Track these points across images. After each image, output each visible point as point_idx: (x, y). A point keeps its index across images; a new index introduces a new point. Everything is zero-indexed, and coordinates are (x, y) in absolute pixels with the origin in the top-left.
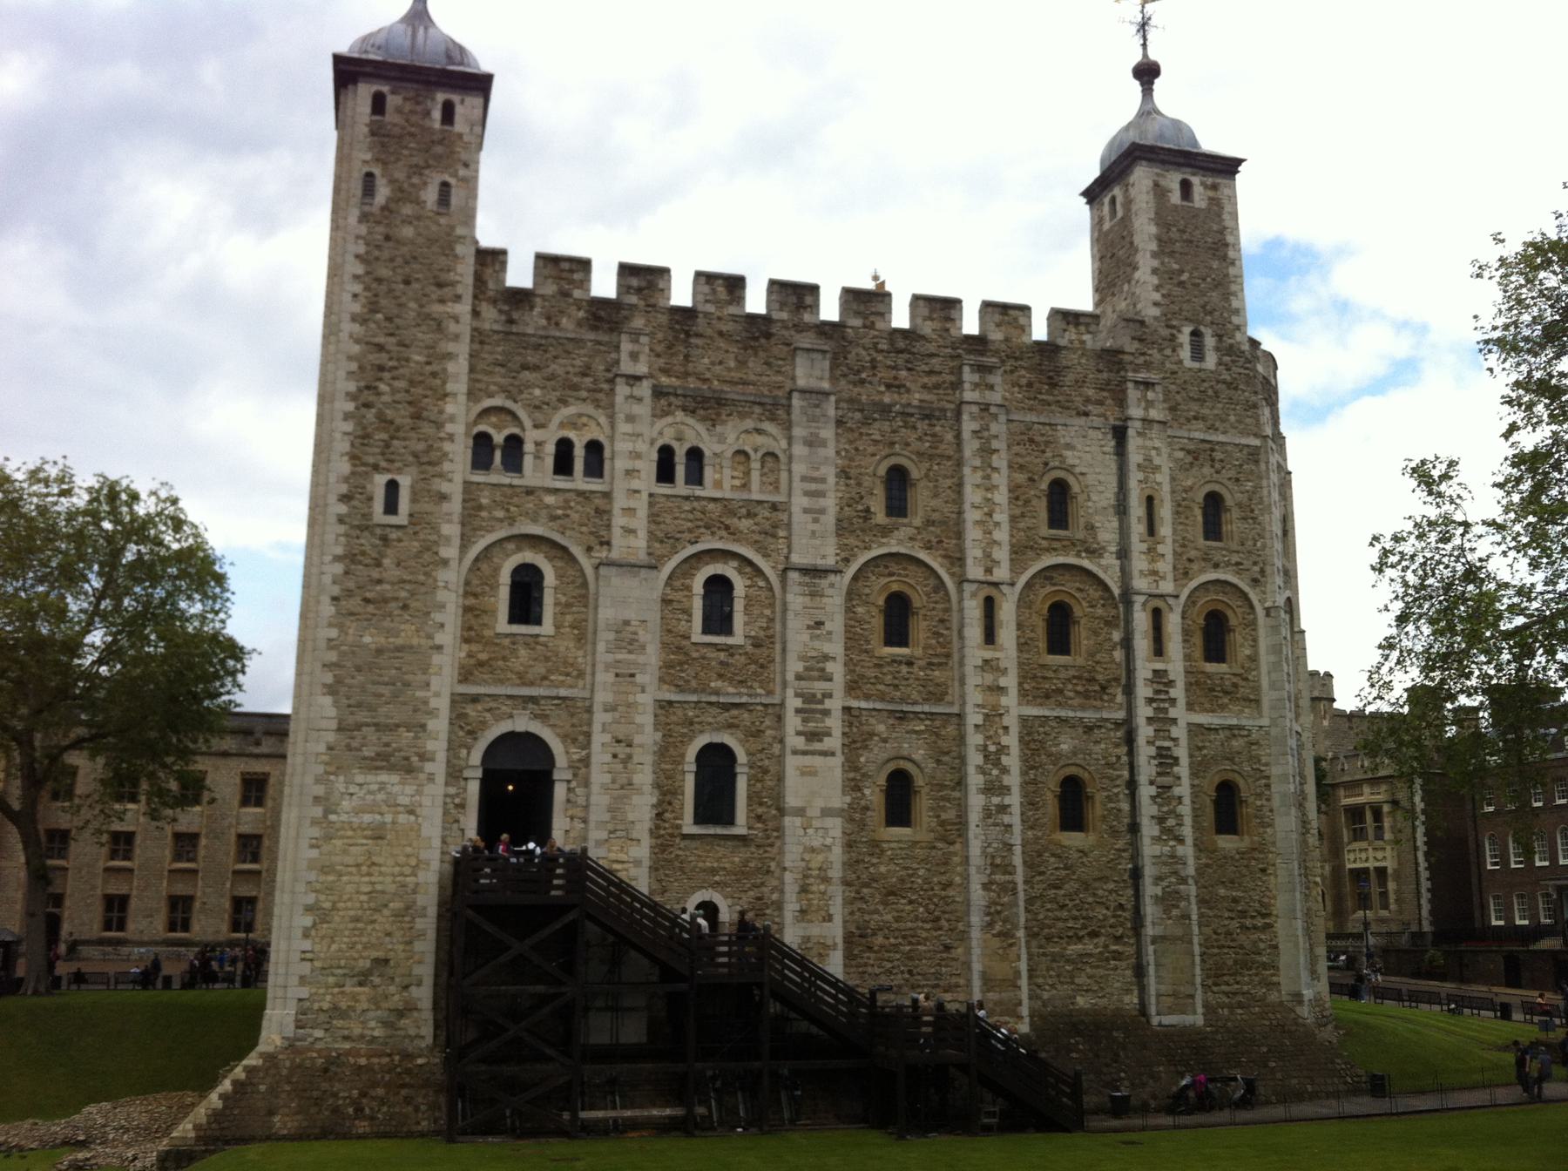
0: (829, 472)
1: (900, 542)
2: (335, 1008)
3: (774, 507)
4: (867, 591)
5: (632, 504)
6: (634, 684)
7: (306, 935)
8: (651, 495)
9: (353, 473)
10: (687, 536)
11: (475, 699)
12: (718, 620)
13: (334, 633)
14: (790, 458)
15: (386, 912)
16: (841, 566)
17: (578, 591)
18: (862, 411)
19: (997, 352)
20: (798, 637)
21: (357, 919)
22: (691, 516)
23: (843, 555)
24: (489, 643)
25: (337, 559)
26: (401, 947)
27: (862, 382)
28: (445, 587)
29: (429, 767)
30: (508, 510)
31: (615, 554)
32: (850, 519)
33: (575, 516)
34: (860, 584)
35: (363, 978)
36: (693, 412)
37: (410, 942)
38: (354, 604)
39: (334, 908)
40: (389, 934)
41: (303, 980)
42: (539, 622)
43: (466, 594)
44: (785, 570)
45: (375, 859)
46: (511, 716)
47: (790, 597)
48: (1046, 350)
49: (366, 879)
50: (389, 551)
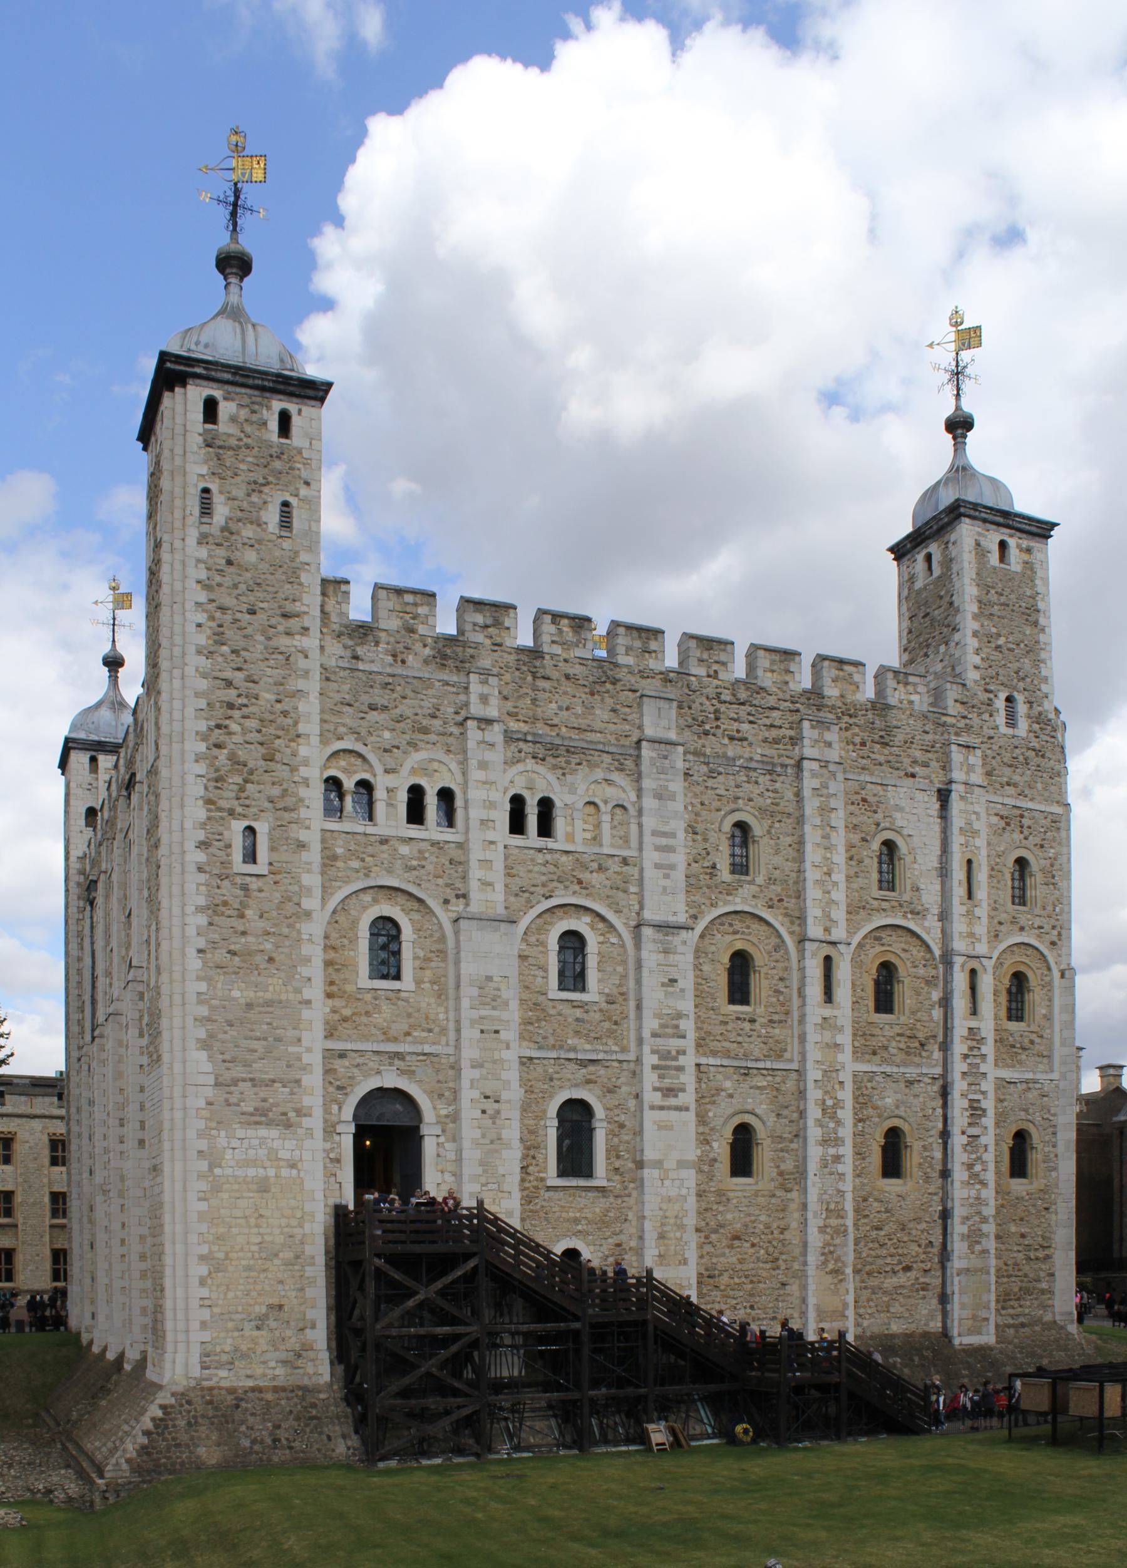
0: (679, 826)
1: (745, 900)
2: (236, 1350)
3: (625, 862)
4: (713, 948)
5: (488, 855)
6: (501, 1042)
7: (202, 1282)
8: (505, 847)
9: (209, 818)
10: (540, 890)
11: (342, 1055)
12: (573, 977)
13: (203, 987)
14: (640, 812)
15: (277, 1262)
16: (690, 922)
17: (435, 947)
18: (707, 764)
19: (833, 707)
20: (653, 994)
21: (249, 1268)
22: (544, 870)
23: (692, 911)
24: (350, 998)
25: (200, 909)
26: (294, 1294)
27: (706, 733)
28: (310, 940)
29: (306, 1122)
30: (363, 860)
31: (474, 908)
32: (696, 876)
33: (430, 868)
34: (707, 941)
35: (260, 1323)
36: (543, 760)
37: (302, 1289)
38: (220, 956)
39: (227, 1258)
40: (281, 1282)
41: (204, 1325)
42: (397, 977)
43: (326, 948)
44: (638, 926)
45: (262, 1211)
46: (379, 1072)
47: (644, 954)
48: (880, 706)
49: (256, 1230)
50: (251, 902)
